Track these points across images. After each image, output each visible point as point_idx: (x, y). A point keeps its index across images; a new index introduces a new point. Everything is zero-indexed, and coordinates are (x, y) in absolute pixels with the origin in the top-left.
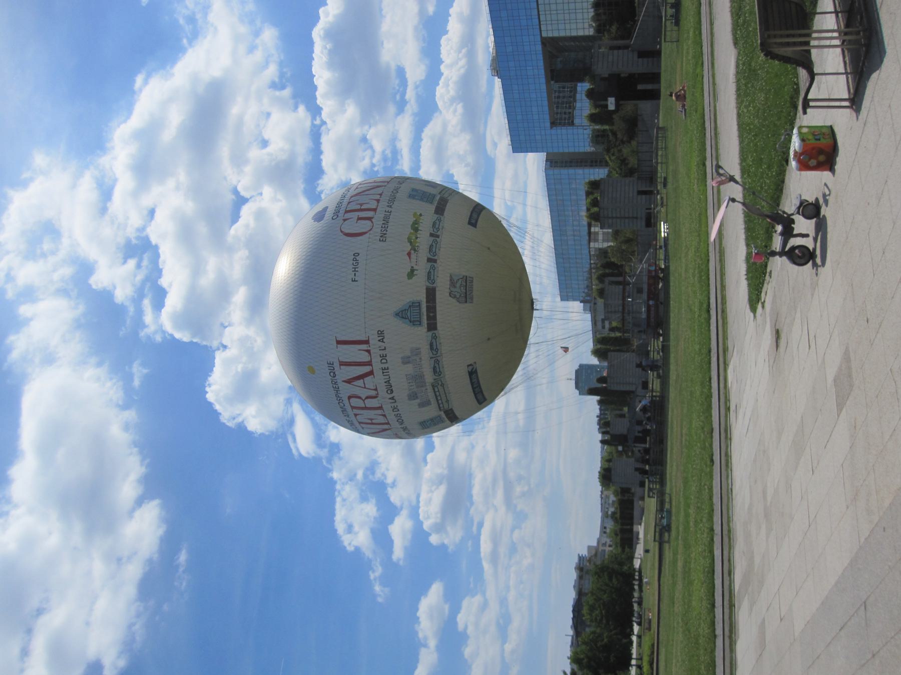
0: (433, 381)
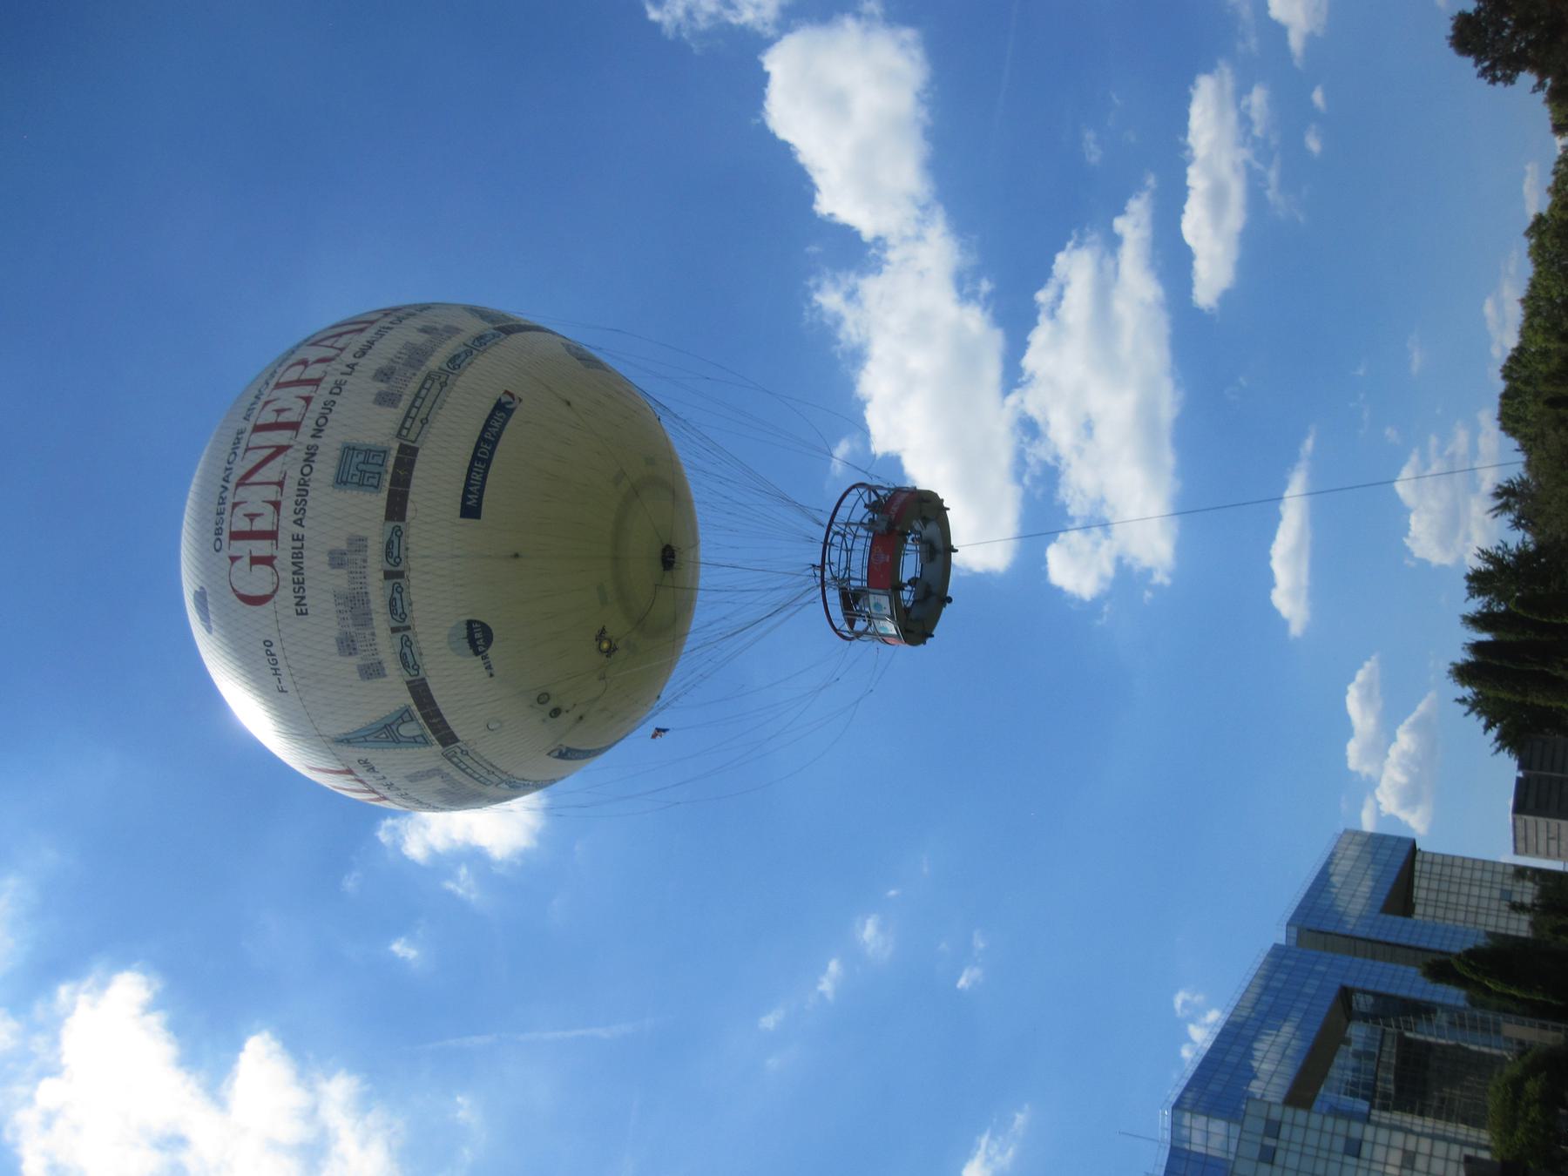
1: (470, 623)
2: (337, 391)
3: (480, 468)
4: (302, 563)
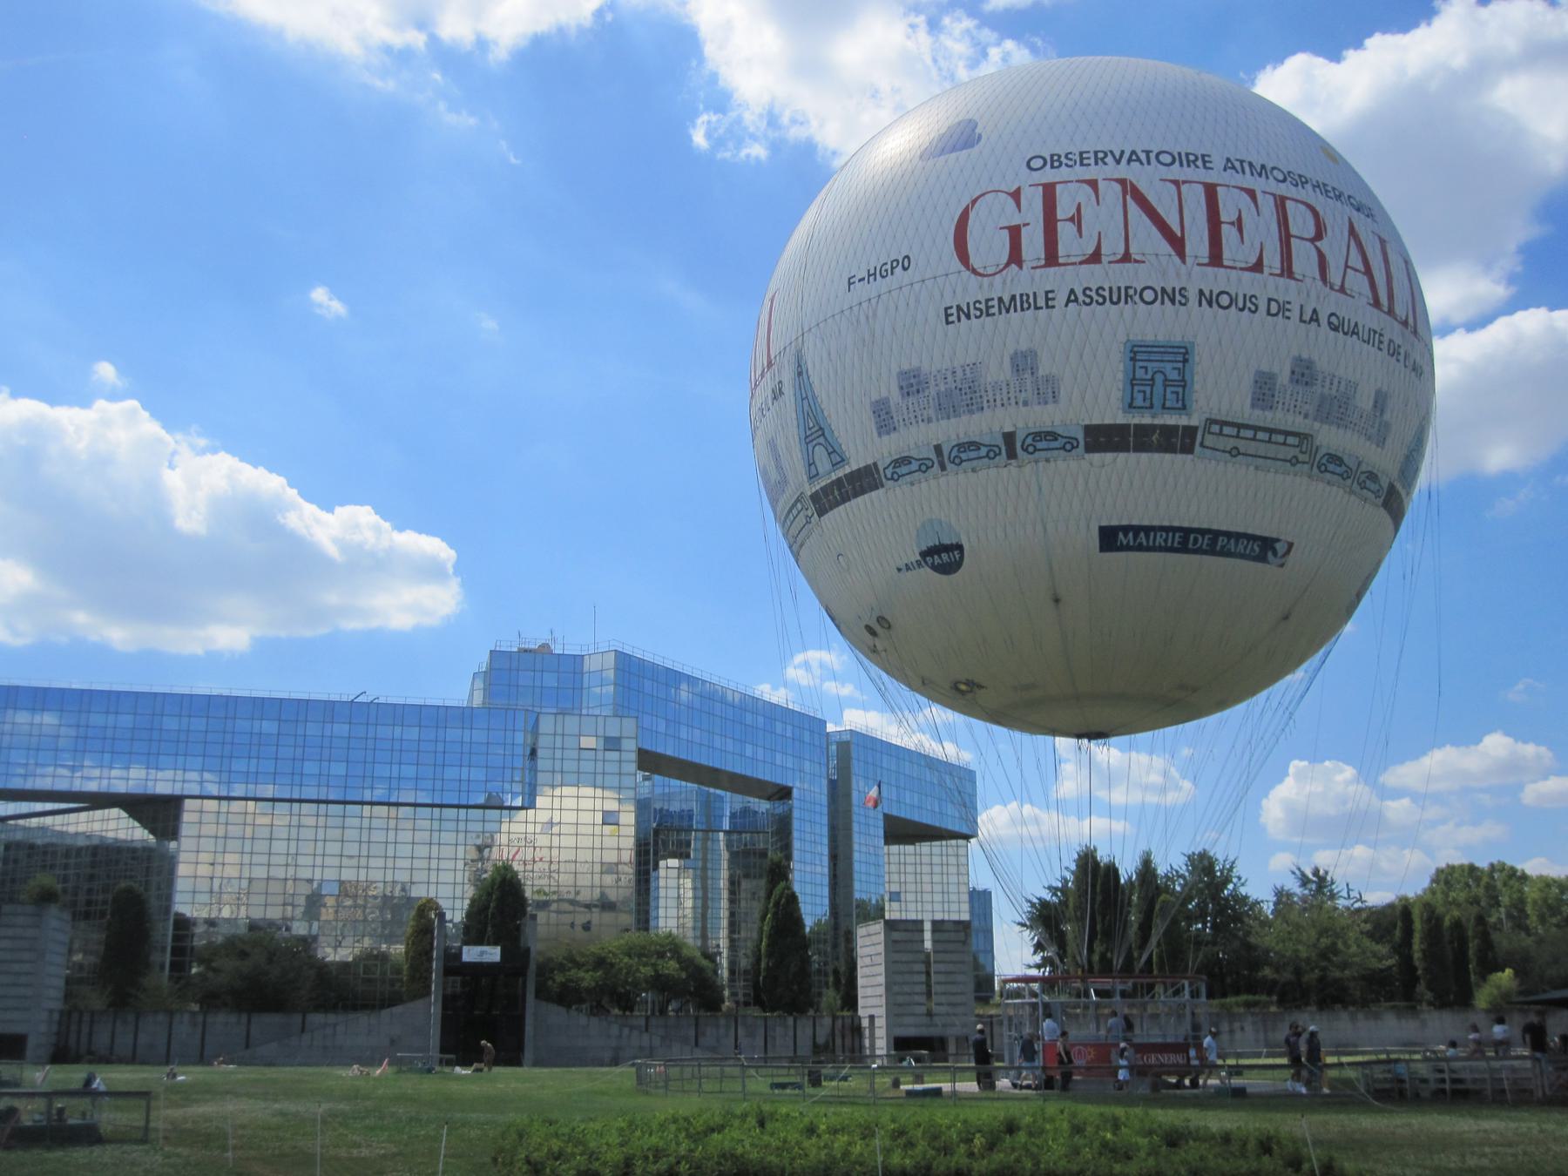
0: (1317, 443)
1: (959, 547)
2: (1274, 309)
3: (1173, 542)
4: (1016, 310)
